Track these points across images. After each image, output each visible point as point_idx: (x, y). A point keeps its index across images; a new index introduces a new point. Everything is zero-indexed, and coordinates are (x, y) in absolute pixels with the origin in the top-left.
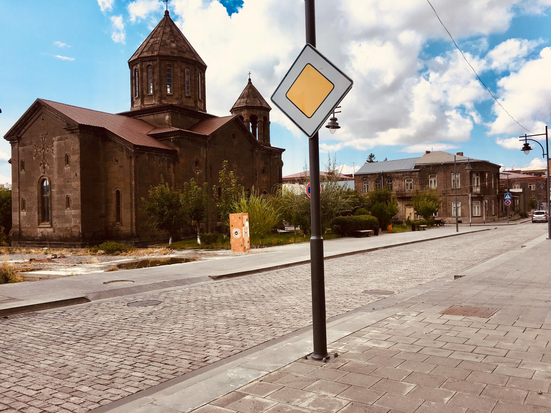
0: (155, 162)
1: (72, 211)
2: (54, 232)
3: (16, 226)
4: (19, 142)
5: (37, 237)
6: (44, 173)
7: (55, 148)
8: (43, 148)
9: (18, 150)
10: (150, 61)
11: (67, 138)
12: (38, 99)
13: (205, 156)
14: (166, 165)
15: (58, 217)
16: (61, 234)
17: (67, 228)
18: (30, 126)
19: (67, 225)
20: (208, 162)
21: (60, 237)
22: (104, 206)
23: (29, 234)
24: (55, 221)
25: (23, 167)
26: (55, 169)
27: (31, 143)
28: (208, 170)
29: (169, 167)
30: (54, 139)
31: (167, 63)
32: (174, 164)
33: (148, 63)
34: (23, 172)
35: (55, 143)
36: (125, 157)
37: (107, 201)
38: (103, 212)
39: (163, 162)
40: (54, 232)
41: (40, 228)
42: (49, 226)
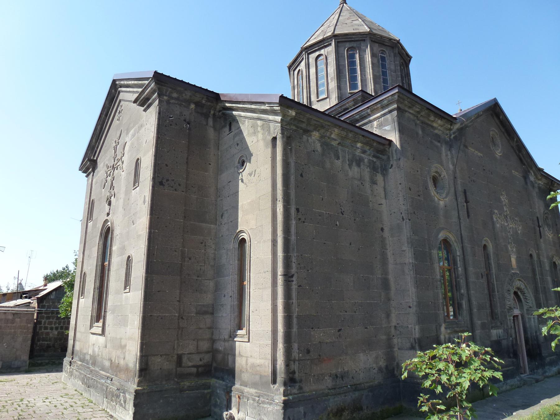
0: (338, 163)
4: (94, 172)
5: (88, 353)
10: (320, 49)
13: (451, 166)
20: (459, 181)
22: (211, 284)
28: (461, 199)
29: (374, 182)
31: (348, 45)
33: (317, 53)
36: (261, 143)
37: (218, 271)
38: (208, 299)
39: (359, 165)
42: (99, 331)
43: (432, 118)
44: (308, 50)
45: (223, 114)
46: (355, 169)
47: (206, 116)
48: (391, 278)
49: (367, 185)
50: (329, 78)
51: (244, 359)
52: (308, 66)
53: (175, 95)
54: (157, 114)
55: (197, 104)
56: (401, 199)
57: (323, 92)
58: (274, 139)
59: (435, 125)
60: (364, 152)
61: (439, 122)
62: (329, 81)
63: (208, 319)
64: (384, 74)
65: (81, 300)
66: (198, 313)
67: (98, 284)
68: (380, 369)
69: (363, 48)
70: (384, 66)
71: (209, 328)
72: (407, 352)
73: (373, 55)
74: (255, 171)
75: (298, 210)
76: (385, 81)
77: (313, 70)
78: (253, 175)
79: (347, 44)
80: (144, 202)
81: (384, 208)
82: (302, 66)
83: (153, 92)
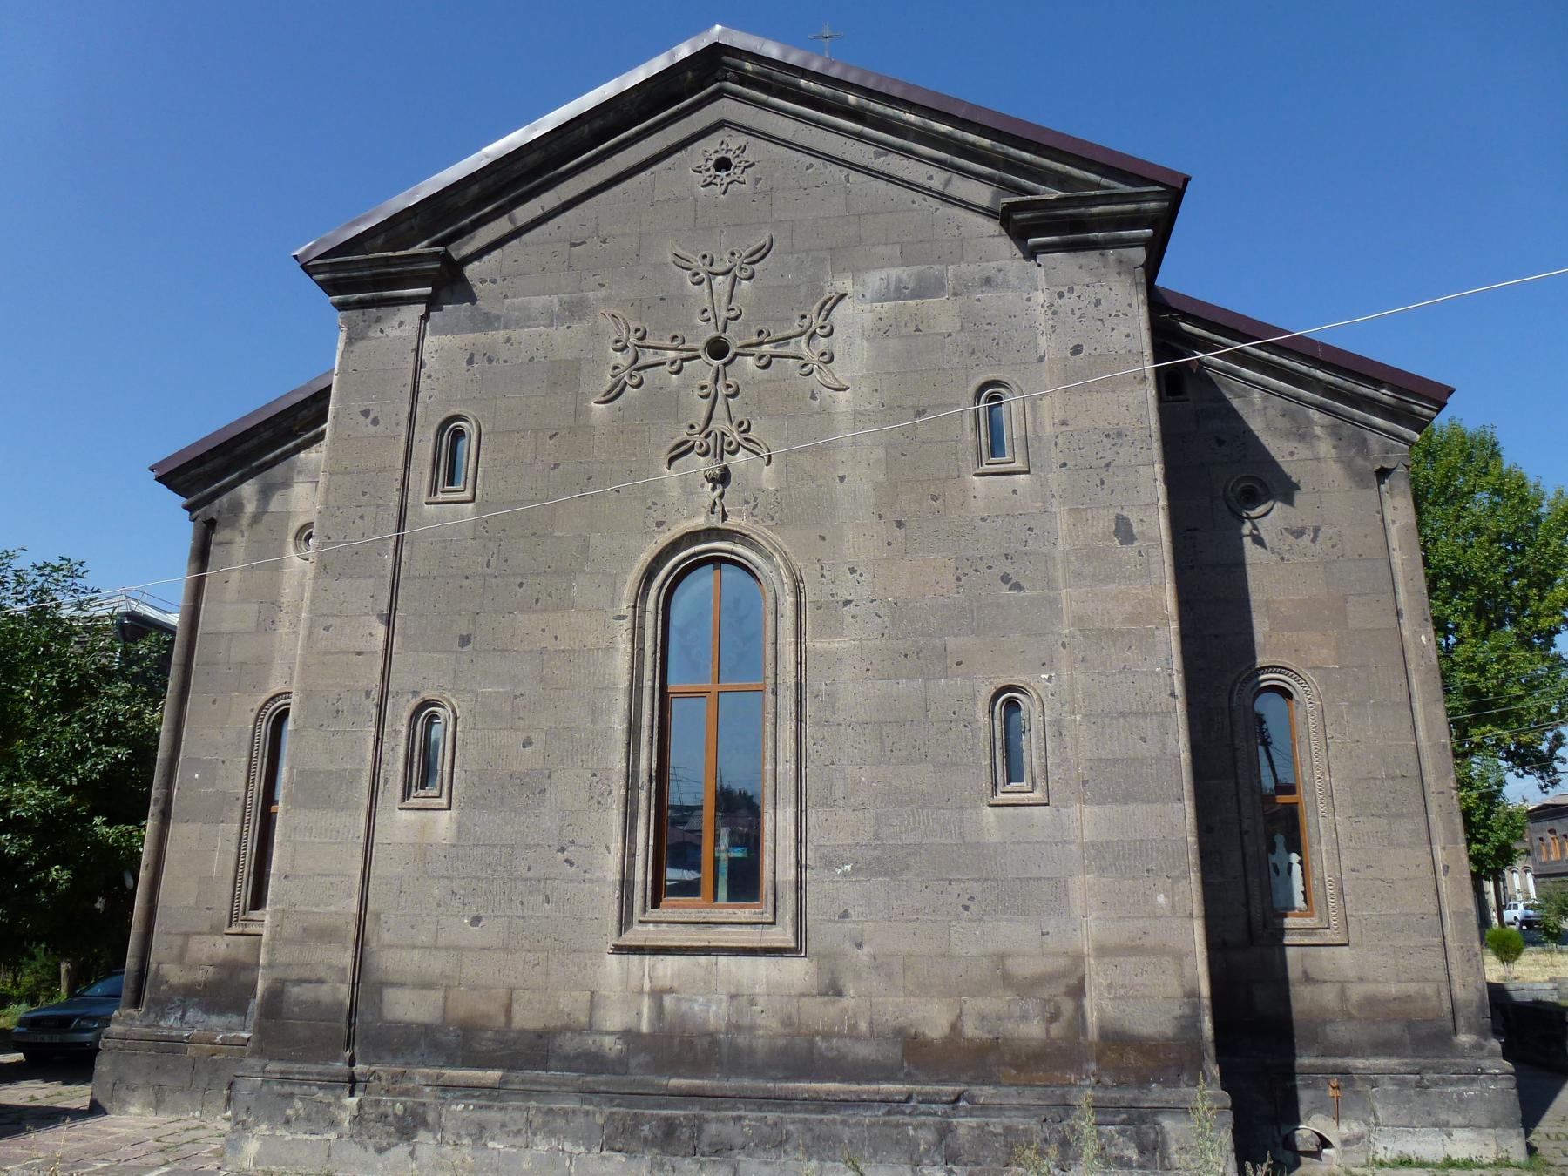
2: (834, 990)
5: (590, 1028)
9: (418, 351)
30: (844, 284)
34: (443, 517)
74: (1316, 530)
78: (1306, 539)
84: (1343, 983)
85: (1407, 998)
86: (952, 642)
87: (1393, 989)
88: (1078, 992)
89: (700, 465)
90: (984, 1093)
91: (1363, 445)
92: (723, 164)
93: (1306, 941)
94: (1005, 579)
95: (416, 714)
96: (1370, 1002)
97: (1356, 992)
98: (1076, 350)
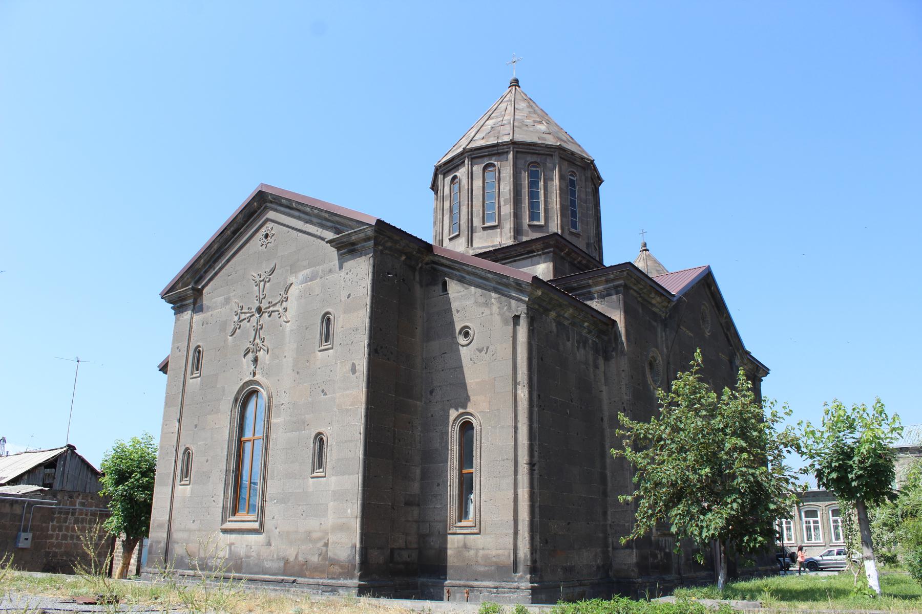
0: (569, 344)
1: (333, 479)
2: (269, 544)
3: (160, 526)
6: (254, 374)
7: (292, 304)
8: (259, 310)
11: (330, 271)
12: (262, 185)
13: (665, 350)
14: (591, 358)
15: (283, 499)
16: (291, 553)
17: (309, 533)
18: (228, 261)
19: (313, 524)
21: (287, 562)
22: (418, 471)
23: (193, 547)
24: (271, 509)
25: (197, 365)
26: (288, 362)
27: (227, 301)
29: (596, 367)
30: (292, 279)
31: (530, 158)
32: (607, 359)
34: (193, 383)
35: (294, 291)
36: (497, 319)
38: (415, 487)
40: (269, 544)
41: (225, 531)
43: (653, 295)
44: (474, 154)
45: (435, 269)
46: (582, 351)
47: (413, 269)
48: (609, 474)
49: (591, 370)
50: (502, 200)
51: (472, 552)
52: (471, 176)
53: (389, 244)
54: (371, 267)
55: (409, 257)
56: (624, 388)
57: (491, 217)
58: (517, 318)
59: (654, 302)
60: (590, 332)
61: (658, 299)
62: (502, 203)
63: (416, 511)
64: (573, 203)
65: (179, 489)
66: (408, 504)
67: (233, 465)
68: (598, 567)
69: (549, 165)
70: (573, 193)
71: (416, 522)
72: (622, 551)
73: (562, 178)
74: (488, 348)
75: (539, 396)
76: (574, 214)
77: (478, 183)
78: (484, 352)
79: (532, 158)
80: (354, 370)
81: (605, 396)
82: (462, 173)
83: (368, 239)
84: (477, 550)
85: (498, 556)
86: (307, 416)
87: (494, 553)
88: (326, 545)
89: (251, 356)
90: (300, 580)
91: (509, 305)
92: (267, 236)
93: (465, 532)
94: (323, 391)
95: (184, 453)
96: (486, 557)
97: (481, 552)
98: (349, 296)
